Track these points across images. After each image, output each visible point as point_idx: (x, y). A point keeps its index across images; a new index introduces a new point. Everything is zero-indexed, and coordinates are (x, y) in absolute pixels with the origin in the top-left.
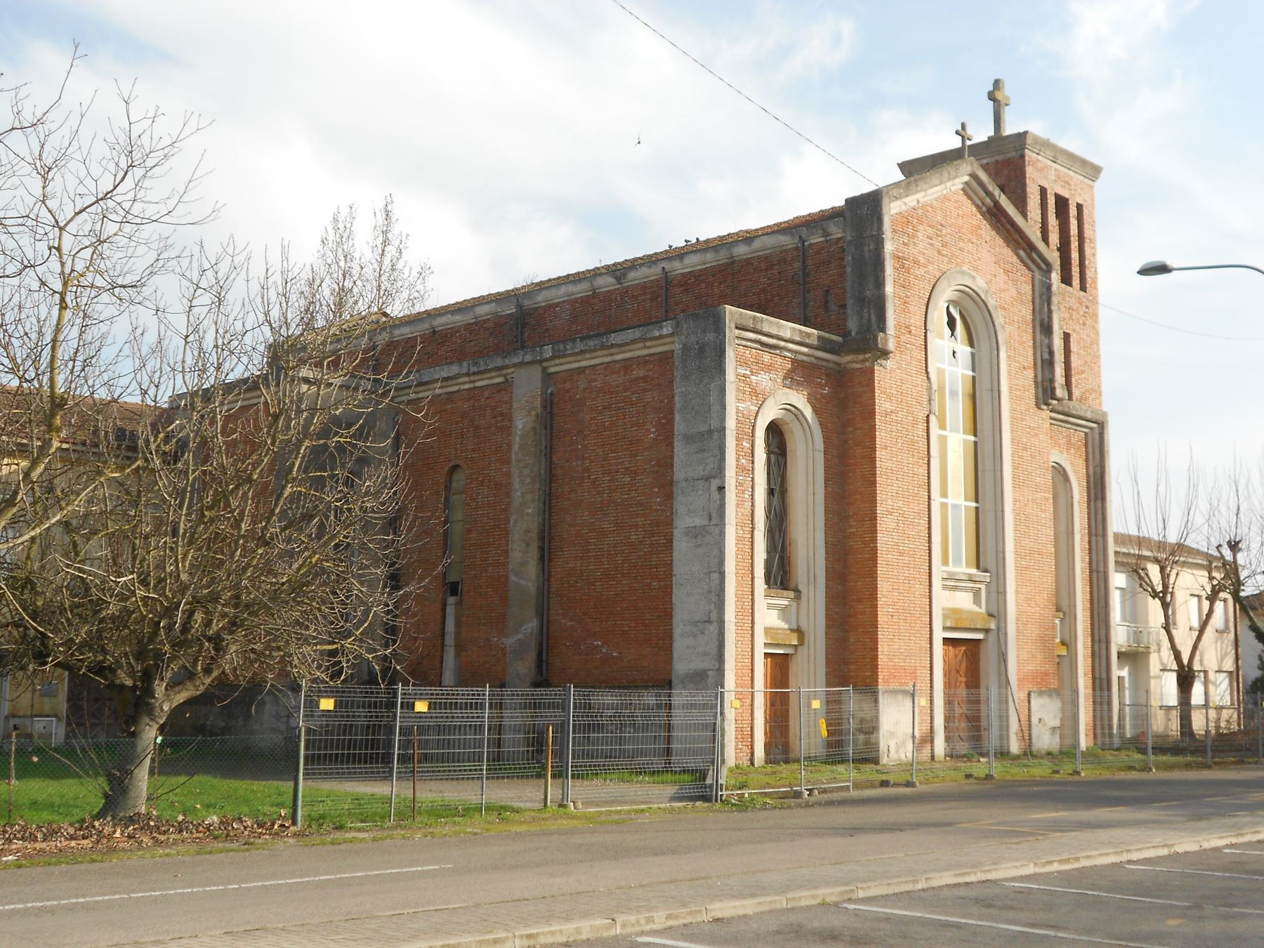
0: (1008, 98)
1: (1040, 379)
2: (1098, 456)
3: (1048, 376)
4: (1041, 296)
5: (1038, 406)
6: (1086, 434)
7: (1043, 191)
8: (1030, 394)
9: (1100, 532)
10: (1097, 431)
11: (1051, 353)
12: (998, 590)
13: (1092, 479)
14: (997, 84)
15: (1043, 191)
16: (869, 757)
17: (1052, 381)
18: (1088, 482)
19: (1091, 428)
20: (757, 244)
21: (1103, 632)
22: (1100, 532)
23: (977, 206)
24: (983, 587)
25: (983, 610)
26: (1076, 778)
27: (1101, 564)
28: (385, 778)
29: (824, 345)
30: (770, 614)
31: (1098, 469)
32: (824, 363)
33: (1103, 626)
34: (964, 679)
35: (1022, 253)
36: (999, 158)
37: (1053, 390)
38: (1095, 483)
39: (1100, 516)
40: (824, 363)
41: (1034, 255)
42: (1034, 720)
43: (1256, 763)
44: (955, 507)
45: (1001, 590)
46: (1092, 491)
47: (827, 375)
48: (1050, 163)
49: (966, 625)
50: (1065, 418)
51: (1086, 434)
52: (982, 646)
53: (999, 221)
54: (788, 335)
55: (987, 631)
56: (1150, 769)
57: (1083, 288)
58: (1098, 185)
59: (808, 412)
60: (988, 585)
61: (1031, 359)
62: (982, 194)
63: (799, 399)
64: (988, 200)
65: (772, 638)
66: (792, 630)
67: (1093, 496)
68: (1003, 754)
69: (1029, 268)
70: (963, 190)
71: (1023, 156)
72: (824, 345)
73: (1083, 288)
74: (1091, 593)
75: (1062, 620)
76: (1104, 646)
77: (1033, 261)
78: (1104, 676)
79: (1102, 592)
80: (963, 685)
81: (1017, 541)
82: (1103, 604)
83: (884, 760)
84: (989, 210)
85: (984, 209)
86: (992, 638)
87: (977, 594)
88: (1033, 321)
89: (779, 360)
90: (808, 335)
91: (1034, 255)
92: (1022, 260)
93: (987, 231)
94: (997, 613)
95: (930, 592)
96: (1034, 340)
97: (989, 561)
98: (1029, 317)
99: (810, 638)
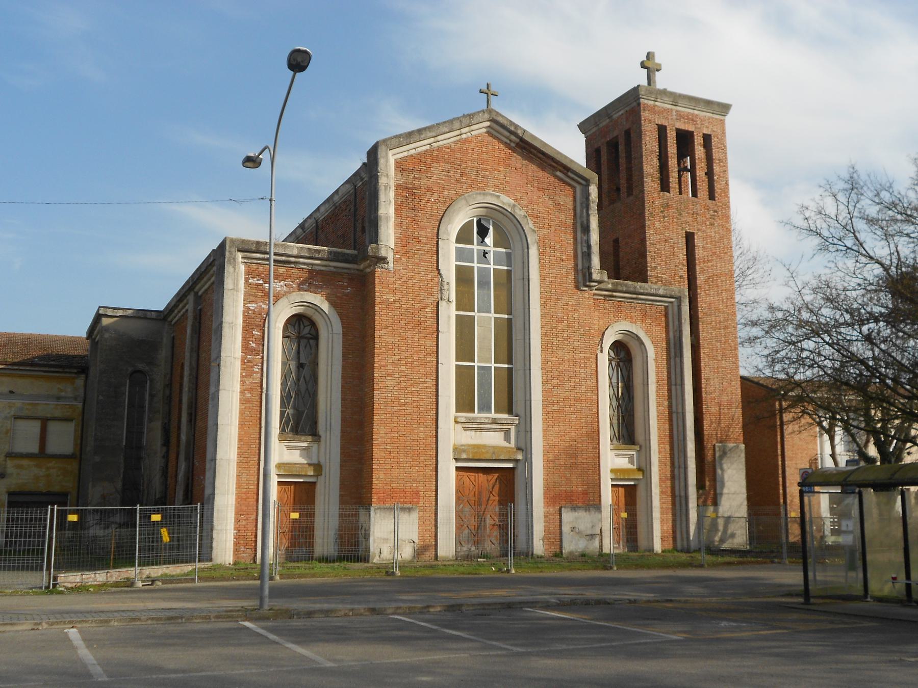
0: (660, 65)
1: (580, 267)
2: (677, 323)
3: (586, 265)
4: (581, 204)
5: (577, 287)
6: (666, 307)
7: (662, 130)
8: (570, 280)
9: (679, 382)
10: (676, 304)
11: (589, 247)
12: (525, 430)
13: (672, 341)
14: (649, 56)
15: (662, 130)
16: (363, 557)
17: (589, 268)
18: (668, 343)
19: (671, 302)
20: (340, 193)
21: (682, 459)
22: (679, 382)
23: (506, 144)
24: (513, 429)
25: (513, 444)
26: (505, 575)
27: (680, 406)
28: (36, 570)
29: (334, 257)
30: (285, 453)
31: (677, 333)
32: (345, 271)
33: (682, 455)
34: (497, 498)
35: (558, 173)
36: (627, 109)
37: (590, 274)
38: (675, 345)
39: (678, 370)
40: (345, 271)
41: (570, 174)
42: (566, 529)
43: (779, 563)
44: (485, 370)
45: (528, 429)
46: (672, 350)
47: (349, 279)
48: (669, 107)
49: (488, 456)
50: (635, 296)
51: (666, 307)
52: (518, 473)
53: (531, 152)
54: (295, 252)
55: (517, 461)
56: (611, 568)
57: (712, 196)
58: (729, 119)
59: (325, 307)
60: (517, 426)
61: (571, 253)
62: (507, 134)
63: (319, 300)
64: (513, 137)
65: (285, 470)
66: (310, 465)
67: (672, 354)
68: (528, 554)
69: (569, 185)
70: (488, 132)
71: (639, 104)
72: (334, 257)
73: (712, 196)
74: (671, 430)
75: (638, 451)
76: (682, 470)
77: (572, 179)
78: (683, 494)
79: (681, 428)
80: (496, 503)
81: (546, 393)
82: (681, 438)
83: (376, 560)
84: (517, 145)
85: (513, 145)
86: (520, 466)
87: (507, 433)
88: (574, 224)
89: (296, 271)
90: (319, 251)
91: (570, 174)
92: (560, 179)
93: (517, 160)
94: (525, 447)
95: (437, 432)
96: (575, 238)
97: (518, 407)
98: (569, 221)
99: (326, 470)
